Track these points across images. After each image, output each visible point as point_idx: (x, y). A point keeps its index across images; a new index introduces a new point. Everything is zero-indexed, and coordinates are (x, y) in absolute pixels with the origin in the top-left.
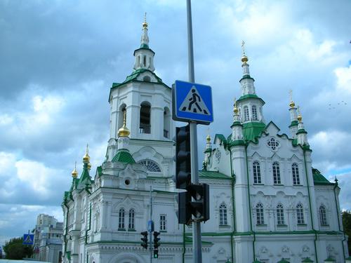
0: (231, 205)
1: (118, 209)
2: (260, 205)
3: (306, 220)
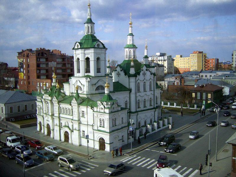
0: (129, 101)
2: (139, 100)
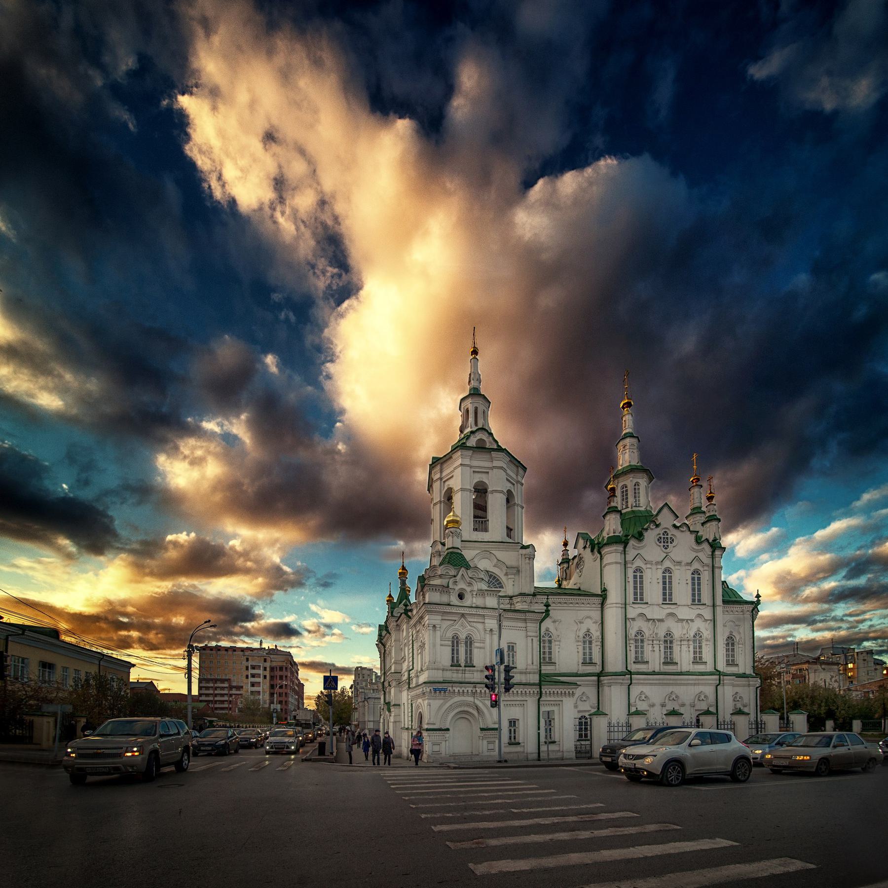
0: (599, 634)
1: (450, 635)
2: (640, 632)
3: (707, 655)
